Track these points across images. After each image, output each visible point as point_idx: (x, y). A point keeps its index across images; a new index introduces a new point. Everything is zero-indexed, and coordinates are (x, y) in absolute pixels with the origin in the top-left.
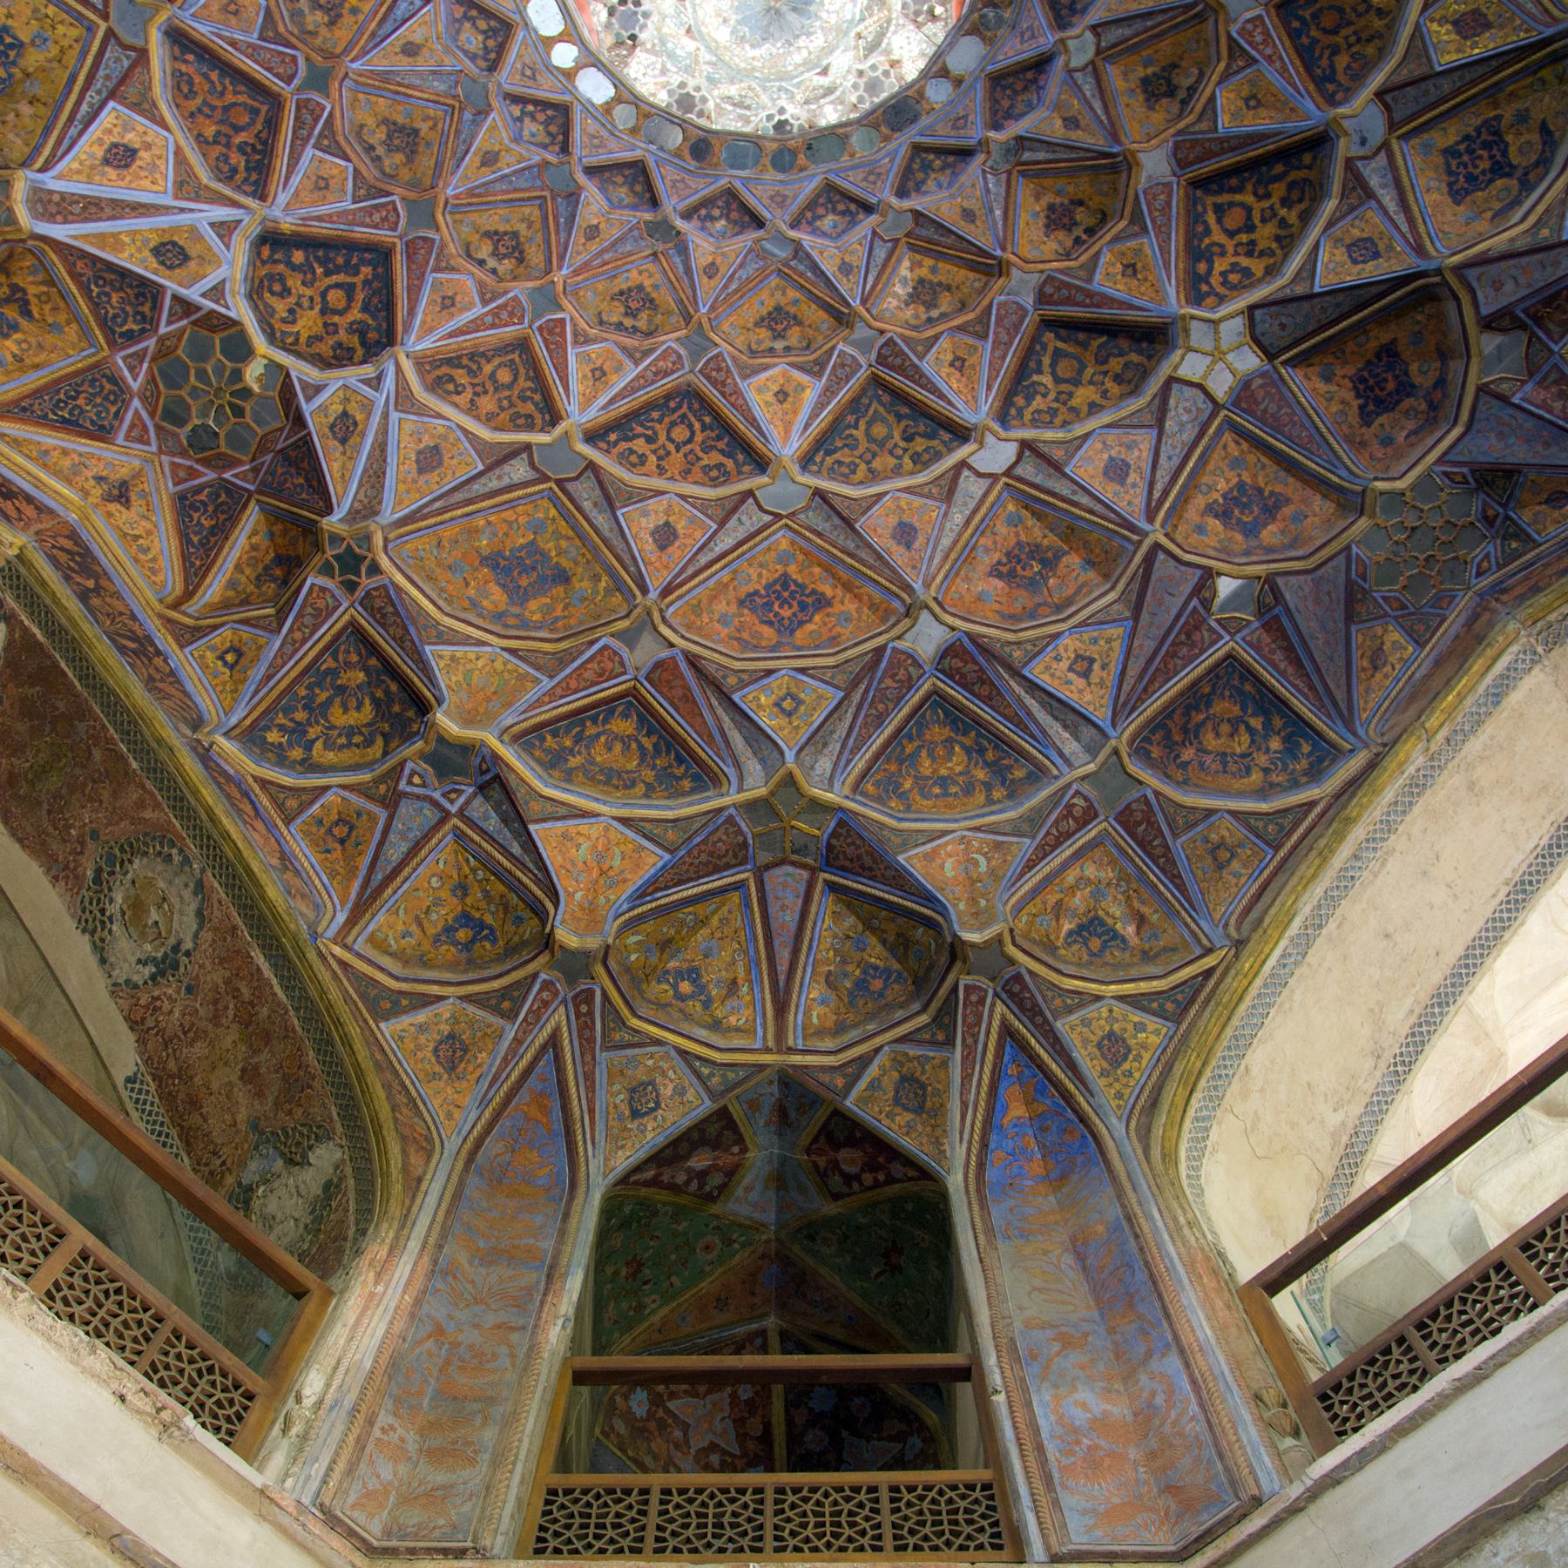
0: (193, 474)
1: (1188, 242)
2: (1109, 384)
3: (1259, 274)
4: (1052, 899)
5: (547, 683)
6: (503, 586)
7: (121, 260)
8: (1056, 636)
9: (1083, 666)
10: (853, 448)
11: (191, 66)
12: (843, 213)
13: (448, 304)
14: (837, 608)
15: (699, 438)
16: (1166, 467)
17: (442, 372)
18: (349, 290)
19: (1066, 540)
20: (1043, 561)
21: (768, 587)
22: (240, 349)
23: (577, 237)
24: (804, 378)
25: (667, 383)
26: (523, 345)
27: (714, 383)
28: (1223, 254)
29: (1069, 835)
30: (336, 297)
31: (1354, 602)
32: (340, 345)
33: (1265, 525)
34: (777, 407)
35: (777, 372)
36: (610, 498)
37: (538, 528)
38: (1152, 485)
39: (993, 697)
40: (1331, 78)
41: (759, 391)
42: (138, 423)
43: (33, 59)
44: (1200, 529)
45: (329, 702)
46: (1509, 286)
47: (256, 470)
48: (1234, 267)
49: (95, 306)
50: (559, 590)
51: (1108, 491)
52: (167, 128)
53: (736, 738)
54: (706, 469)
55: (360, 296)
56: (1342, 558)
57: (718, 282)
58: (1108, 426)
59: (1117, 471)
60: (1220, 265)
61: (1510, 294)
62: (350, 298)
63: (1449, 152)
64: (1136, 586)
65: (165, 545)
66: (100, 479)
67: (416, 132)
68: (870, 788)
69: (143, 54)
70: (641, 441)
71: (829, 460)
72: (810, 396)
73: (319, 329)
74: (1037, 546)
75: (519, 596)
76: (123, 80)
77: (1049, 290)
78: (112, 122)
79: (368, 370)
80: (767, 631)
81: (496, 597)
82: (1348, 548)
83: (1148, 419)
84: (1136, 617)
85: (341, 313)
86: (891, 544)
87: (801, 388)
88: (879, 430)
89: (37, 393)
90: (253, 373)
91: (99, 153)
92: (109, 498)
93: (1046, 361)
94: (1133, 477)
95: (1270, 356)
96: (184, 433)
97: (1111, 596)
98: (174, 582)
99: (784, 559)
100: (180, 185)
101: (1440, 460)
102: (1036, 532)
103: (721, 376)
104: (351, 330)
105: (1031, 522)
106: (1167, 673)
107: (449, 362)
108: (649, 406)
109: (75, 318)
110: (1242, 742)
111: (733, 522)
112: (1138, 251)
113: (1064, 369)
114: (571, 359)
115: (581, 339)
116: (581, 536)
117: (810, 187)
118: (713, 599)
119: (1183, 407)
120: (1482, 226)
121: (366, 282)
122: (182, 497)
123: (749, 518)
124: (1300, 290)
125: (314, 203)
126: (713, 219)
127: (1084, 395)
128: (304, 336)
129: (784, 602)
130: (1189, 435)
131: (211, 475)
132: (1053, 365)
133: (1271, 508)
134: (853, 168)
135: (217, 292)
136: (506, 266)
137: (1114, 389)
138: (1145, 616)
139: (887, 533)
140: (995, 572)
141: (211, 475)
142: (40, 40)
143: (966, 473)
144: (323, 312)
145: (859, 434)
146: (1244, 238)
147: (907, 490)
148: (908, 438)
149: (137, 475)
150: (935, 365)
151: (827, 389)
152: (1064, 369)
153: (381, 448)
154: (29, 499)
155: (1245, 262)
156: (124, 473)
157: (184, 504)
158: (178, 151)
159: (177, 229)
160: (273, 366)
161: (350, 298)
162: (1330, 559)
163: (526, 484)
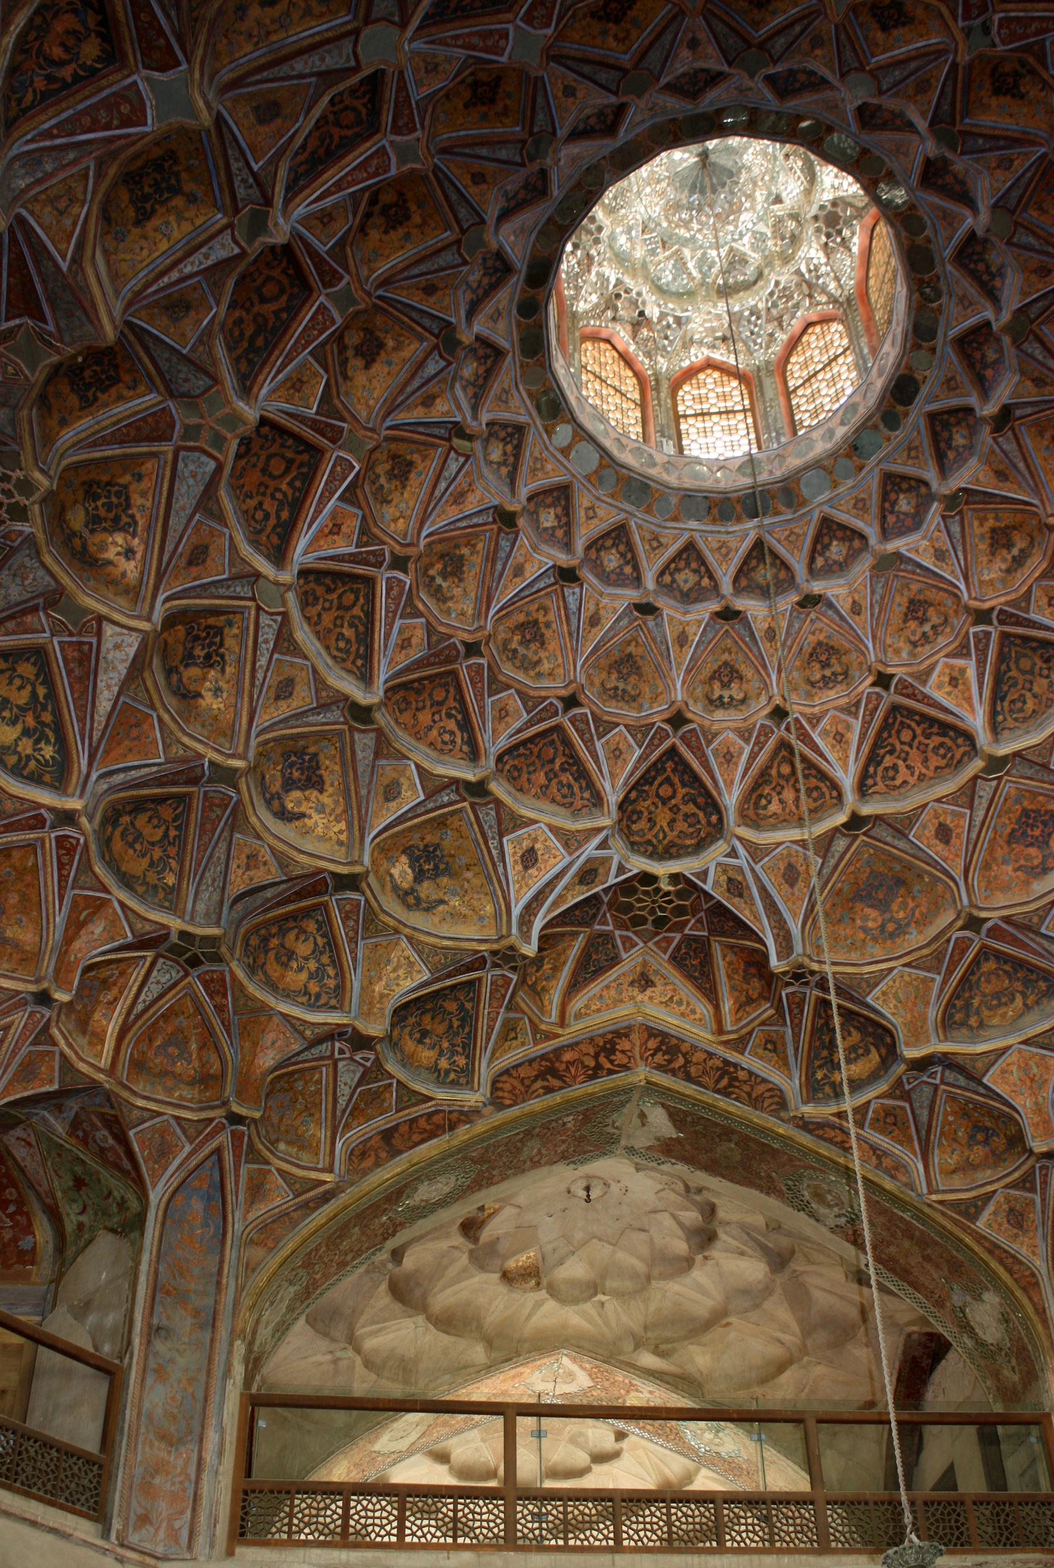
10: (1015, 685)
13: (728, 758)
15: (918, 731)
18: (668, 780)
24: (960, 662)
25: (880, 714)
27: (908, 696)
30: (665, 791)
32: (686, 816)
41: (939, 687)
43: (446, 844)
52: (536, 822)
54: (935, 749)
55: (676, 780)
62: (672, 785)
70: (888, 758)
71: (1006, 704)
72: (971, 673)
73: (669, 815)
76: (500, 823)
85: (673, 797)
87: (963, 671)
88: (1025, 664)
103: (910, 691)
104: (685, 802)
107: (753, 789)
108: (879, 734)
114: (818, 740)
115: (815, 720)
121: (674, 770)
125: (623, 768)
128: (665, 824)
144: (664, 804)
151: (978, 661)
158: (552, 828)
161: (672, 785)
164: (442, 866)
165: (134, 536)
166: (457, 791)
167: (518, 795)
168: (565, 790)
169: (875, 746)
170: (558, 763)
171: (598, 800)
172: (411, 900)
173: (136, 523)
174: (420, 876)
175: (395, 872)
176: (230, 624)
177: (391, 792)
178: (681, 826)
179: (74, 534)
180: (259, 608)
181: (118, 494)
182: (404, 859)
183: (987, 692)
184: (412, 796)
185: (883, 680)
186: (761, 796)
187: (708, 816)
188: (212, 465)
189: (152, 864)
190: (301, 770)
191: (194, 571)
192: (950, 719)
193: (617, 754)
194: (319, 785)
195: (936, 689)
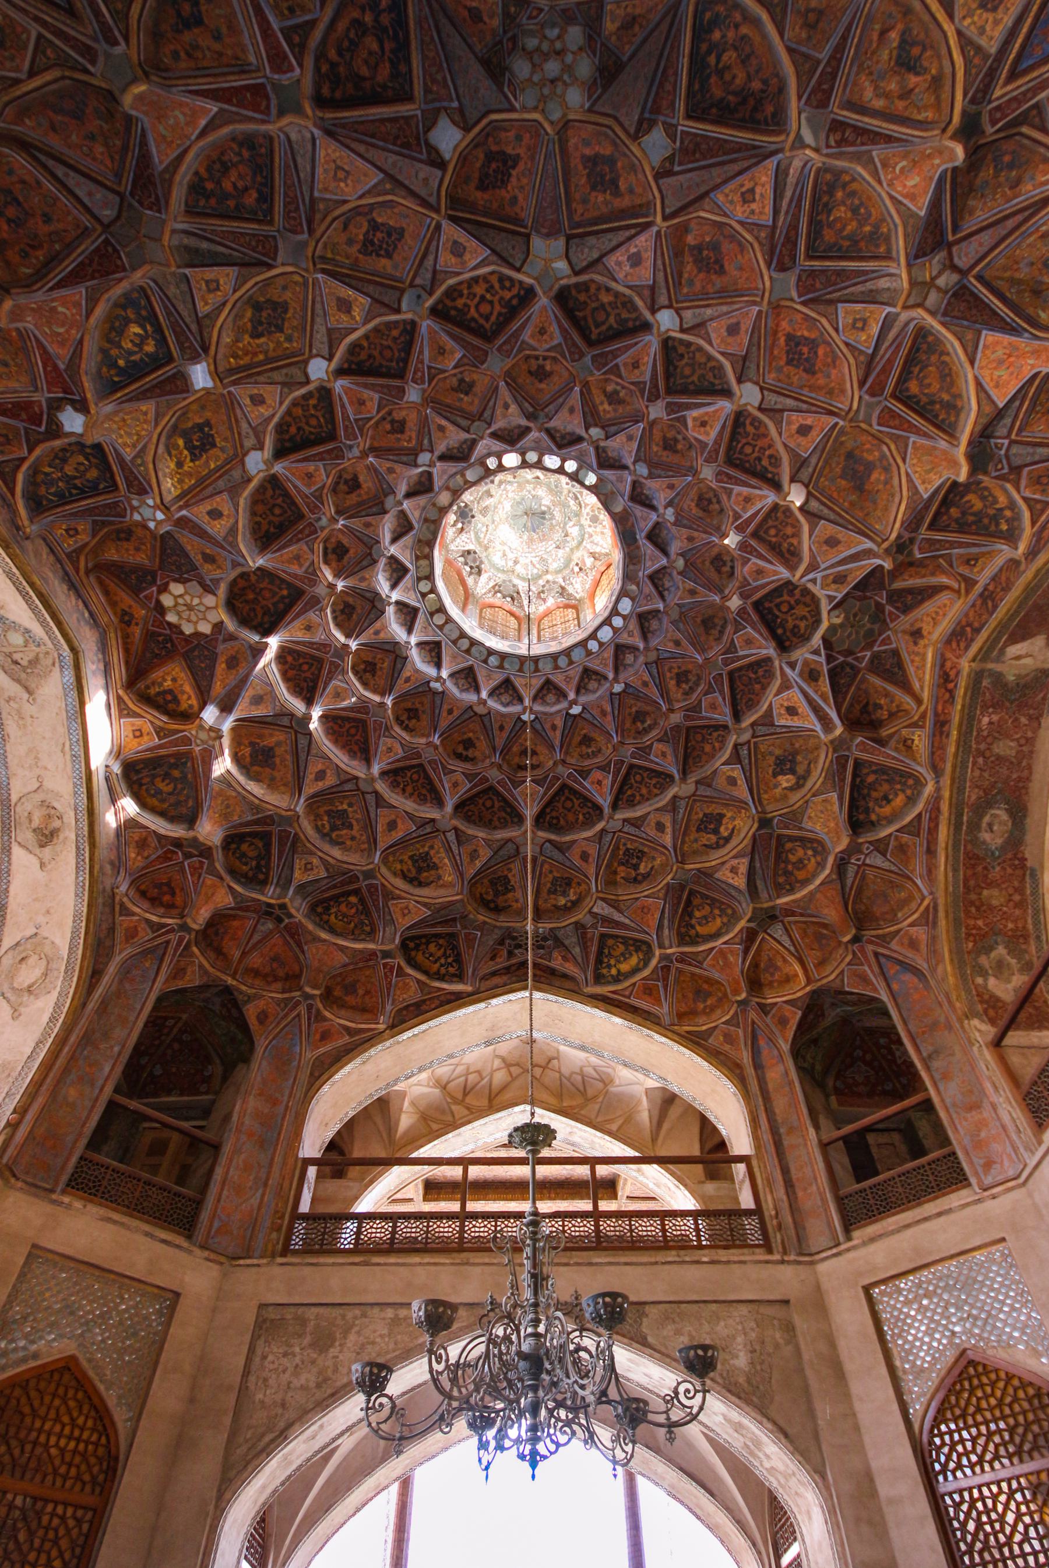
7: (827, 689)
11: (742, 706)
13: (760, 572)
14: (789, 329)
17: (789, 556)
18: (778, 606)
19: (682, 253)
22: (832, 628)
26: (755, 535)
29: (855, 128)
30: (784, 608)
35: (693, 433)
40: (405, 330)
41: (707, 434)
42: (883, 643)
43: (778, 752)
44: (631, 191)
46: (421, 175)
48: (503, 287)
49: (850, 686)
51: (649, 256)
57: (674, 480)
59: (636, 260)
61: (425, 170)
63: (389, 256)
69: (753, 725)
72: (695, 413)
74: (695, 262)
78: (783, 720)
79: (810, 586)
80: (821, 352)
83: (600, 267)
87: (695, 419)
88: (687, 371)
89: (896, 683)
90: (837, 621)
92: (922, 637)
93: (604, 328)
94: (633, 250)
96: (876, 627)
99: (780, 370)
102: (689, 268)
106: (722, 146)
109: (858, 689)
112: (532, 336)
113: (601, 316)
115: (737, 516)
116: (826, 462)
123: (772, 399)
124: (494, 258)
129: (801, 354)
130: (592, 240)
131: (888, 608)
135: (816, 652)
138: (703, 189)
140: (721, 271)
141: (888, 608)
142: (771, 753)
145: (695, 378)
147: (711, 344)
148: (682, 356)
149: (904, 632)
152: (601, 316)
153: (841, 563)
154: (942, 666)
157: (906, 609)
169: (754, 474)
171: (768, 660)
174: (792, 771)
175: (785, 785)
177: (732, 781)
184: (736, 772)
192: (729, 423)
193: (749, 642)
195: (710, 436)
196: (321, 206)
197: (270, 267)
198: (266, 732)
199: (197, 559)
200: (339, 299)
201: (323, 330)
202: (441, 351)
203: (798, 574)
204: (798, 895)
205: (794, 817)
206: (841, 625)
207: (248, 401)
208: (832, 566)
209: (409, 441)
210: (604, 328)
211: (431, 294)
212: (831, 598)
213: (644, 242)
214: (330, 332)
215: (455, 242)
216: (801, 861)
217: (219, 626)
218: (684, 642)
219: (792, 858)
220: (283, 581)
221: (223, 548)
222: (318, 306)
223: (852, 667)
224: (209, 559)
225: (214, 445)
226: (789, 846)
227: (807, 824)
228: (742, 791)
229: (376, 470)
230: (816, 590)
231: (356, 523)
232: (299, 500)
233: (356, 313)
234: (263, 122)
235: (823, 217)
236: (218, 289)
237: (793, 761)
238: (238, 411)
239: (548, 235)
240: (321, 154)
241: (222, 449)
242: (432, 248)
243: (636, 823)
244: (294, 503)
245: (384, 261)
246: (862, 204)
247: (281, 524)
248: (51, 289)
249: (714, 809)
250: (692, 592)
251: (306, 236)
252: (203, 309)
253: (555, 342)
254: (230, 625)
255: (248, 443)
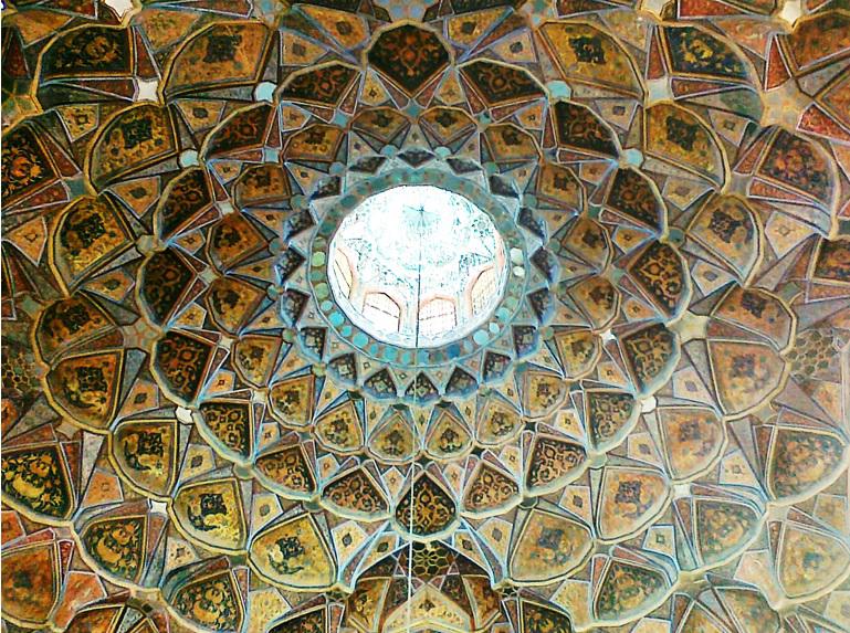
0: (440, 580)
1: (647, 289)
2: (662, 344)
3: (678, 282)
4: (789, 559)
5: (590, 584)
6: (547, 547)
8: (720, 463)
9: (737, 469)
11: (333, 491)
12: (528, 332)
13: (455, 477)
15: (556, 450)
16: (705, 375)
17: (473, 499)
18: (425, 493)
20: (693, 426)
21: (619, 490)
23: (466, 418)
24: (568, 411)
25: (533, 444)
26: (484, 467)
28: (661, 283)
31: (807, 387)
32: (438, 511)
33: (753, 367)
34: (570, 427)
36: (553, 500)
37: (541, 523)
38: (706, 386)
39: (717, 494)
43: (300, 537)
44: (734, 386)
45: (538, 627)
46: (773, 279)
47: (454, 567)
50: (563, 536)
53: (658, 561)
54: (567, 459)
55: (430, 492)
56: (790, 380)
57: (516, 394)
58: (677, 370)
59: (691, 387)
60: (664, 287)
61: (775, 281)
64: (731, 437)
65: (453, 608)
66: (421, 607)
67: (396, 431)
68: (706, 548)
69: (325, 511)
72: (576, 416)
74: (687, 423)
75: (554, 546)
76: (327, 521)
77: (616, 331)
79: (456, 524)
80: (631, 505)
81: (550, 554)
82: (789, 376)
83: (687, 363)
84: (740, 447)
85: (430, 501)
86: (643, 456)
88: (604, 407)
89: (386, 603)
90: (430, 548)
91: (342, 545)
93: (635, 349)
94: (698, 387)
95: (708, 315)
97: (727, 441)
98: (464, 617)
99: (616, 477)
100: (367, 531)
101: (797, 333)
105: (678, 416)
110: (806, 453)
111: (592, 481)
112: (634, 303)
115: (498, 452)
117: (509, 333)
118: (607, 509)
119: (695, 352)
120: (745, 248)
122: (443, 590)
123: (596, 475)
126: (492, 366)
127: (657, 352)
129: (628, 492)
130: (703, 357)
131: (443, 577)
132: (638, 348)
133: (751, 361)
134: (517, 314)
135: (401, 542)
136: (456, 443)
137: (666, 345)
138: (742, 444)
139: (638, 453)
141: (443, 577)
143: (645, 416)
145: (600, 412)
146: (662, 273)
148: (616, 403)
149: (427, 595)
150: (604, 379)
153: (482, 544)
155: (671, 280)
156: (424, 599)
159: (377, 542)
160: (434, 543)
161: (428, 495)
162: (786, 383)
163: (527, 517)
164: (300, 549)
165: (106, 391)
166: (302, 508)
167: (339, 507)
168: (367, 503)
169: (533, 461)
170: (362, 489)
171: (384, 506)
172: (282, 568)
173: (106, 386)
175: (272, 554)
176: (164, 431)
177: (264, 511)
178: (436, 516)
179: (73, 393)
180: (179, 422)
181: (97, 373)
182: (278, 547)
183: (587, 424)
185: (530, 426)
186: (476, 496)
187: (449, 509)
188: (144, 355)
189: (123, 557)
190: (213, 503)
191: (138, 406)
194: (224, 510)
195: (559, 426)
196: (766, 212)
197: (732, 167)
198: (256, 57)
199: (470, 17)
200: (688, 190)
201: (665, 172)
202: (628, 237)
203: (467, 514)
204: (182, 622)
205: (253, 581)
206: (426, 552)
207: (620, 104)
208: (478, 539)
209: (547, 190)
210: (635, 349)
211: (679, 249)
212: (449, 540)
213: (703, 396)
214: (664, 177)
215: (716, 276)
216: (210, 603)
217: (384, 16)
218: (375, 422)
219: (209, 595)
220: (427, 75)
221: (480, 46)
222: (686, 175)
223: (392, 570)
224: (468, 28)
225: (579, 60)
226: (220, 586)
227: (251, 596)
228: (258, 523)
229: (525, 163)
230: (454, 527)
231: (476, 139)
232: (507, 103)
233: (674, 198)
234: (838, 211)
235: (721, 509)
236: (725, 126)
237: (297, 553)
238: (612, 95)
239: (707, 328)
240: (803, 225)
241: (575, 65)
242: (713, 261)
243: (194, 436)
244: (505, 98)
245: (707, 223)
246: (729, 531)
247: (487, 84)
248: (774, 39)
249: (229, 503)
250: (422, 421)
251: (748, 196)
252: (713, 113)
253: (628, 317)
254: (387, 27)
255: (579, 90)
